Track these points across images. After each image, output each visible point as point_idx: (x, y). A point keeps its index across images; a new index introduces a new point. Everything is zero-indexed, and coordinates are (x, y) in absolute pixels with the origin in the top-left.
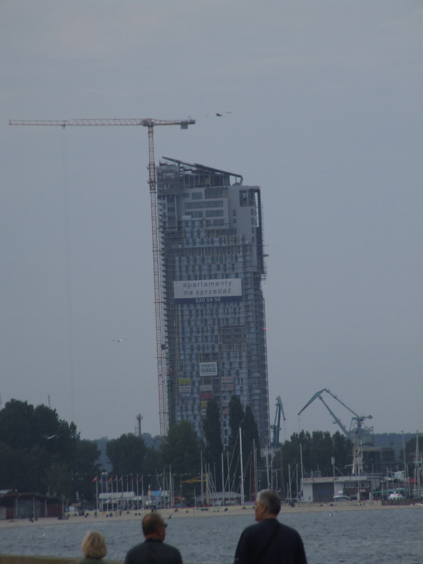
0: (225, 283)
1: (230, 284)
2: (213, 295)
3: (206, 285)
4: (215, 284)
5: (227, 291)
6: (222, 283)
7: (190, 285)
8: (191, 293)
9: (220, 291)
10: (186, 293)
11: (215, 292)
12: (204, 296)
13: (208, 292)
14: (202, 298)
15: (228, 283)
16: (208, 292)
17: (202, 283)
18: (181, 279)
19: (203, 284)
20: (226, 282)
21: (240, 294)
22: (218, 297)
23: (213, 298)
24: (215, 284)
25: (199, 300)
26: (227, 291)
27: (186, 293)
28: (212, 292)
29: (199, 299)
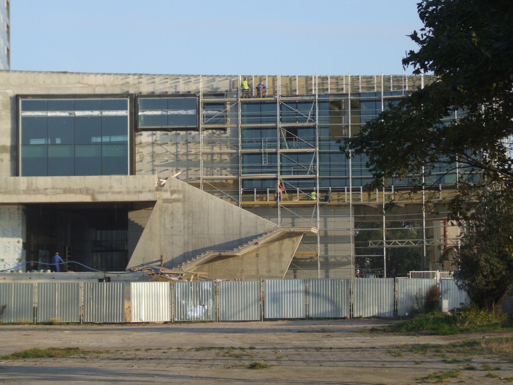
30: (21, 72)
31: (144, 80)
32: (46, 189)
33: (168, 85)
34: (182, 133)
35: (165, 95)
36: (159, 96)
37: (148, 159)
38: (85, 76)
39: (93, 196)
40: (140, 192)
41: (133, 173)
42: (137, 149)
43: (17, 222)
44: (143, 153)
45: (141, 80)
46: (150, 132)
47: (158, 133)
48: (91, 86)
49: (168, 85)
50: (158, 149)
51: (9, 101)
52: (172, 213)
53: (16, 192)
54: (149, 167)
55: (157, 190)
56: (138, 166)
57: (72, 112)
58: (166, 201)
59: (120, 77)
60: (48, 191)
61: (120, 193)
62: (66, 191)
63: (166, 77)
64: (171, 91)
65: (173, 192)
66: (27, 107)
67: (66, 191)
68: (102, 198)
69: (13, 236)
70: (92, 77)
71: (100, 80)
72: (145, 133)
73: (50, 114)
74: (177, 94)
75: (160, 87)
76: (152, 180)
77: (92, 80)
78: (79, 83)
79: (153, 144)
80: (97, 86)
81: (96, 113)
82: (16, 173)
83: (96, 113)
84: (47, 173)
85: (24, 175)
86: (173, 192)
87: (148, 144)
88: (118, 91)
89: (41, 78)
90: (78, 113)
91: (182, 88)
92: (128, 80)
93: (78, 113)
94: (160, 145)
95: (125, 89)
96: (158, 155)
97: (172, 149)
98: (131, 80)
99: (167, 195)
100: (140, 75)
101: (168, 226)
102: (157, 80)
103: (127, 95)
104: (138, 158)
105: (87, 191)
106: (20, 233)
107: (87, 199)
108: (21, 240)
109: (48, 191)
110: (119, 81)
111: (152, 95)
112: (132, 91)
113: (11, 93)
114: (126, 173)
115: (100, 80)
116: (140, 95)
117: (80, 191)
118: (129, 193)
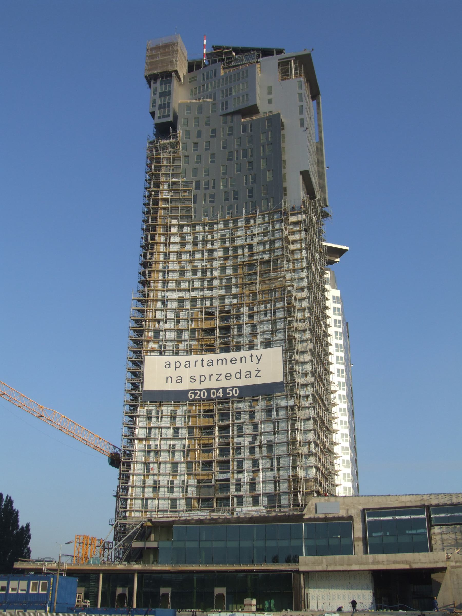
0: (248, 359)
1: (259, 361)
2: (224, 383)
3: (211, 363)
4: (229, 361)
5: (254, 374)
6: (243, 359)
7: (178, 365)
8: (180, 380)
9: (238, 376)
10: (169, 379)
11: (228, 376)
12: (206, 385)
13: (214, 378)
14: (200, 390)
15: (254, 359)
16: (214, 378)
17: (202, 360)
18: (161, 352)
19: (205, 363)
20: (251, 356)
21: (280, 379)
22: (233, 388)
23: (224, 389)
24: (229, 361)
25: (195, 394)
26: (254, 374)
27: (169, 379)
28: (223, 377)
29: (194, 392)
30: (366, 496)
31: (433, 497)
32: (383, 561)
33: (447, 499)
34: (458, 526)
35: (445, 505)
36: (442, 505)
37: (439, 542)
38: (400, 497)
39: (410, 565)
40: (437, 562)
41: (432, 551)
42: (433, 537)
43: (369, 581)
44: (436, 539)
45: (431, 497)
46: (439, 527)
47: (444, 527)
48: (403, 502)
49: (447, 499)
50: (445, 537)
51: (360, 513)
52: (457, 575)
53: (367, 563)
54: (441, 547)
55: (447, 560)
56: (434, 547)
57: (395, 517)
58: (453, 567)
59: (419, 496)
60: (385, 563)
61: (425, 563)
62: (395, 562)
63: (445, 495)
64: (448, 502)
65: (456, 562)
66: (370, 515)
67: (395, 562)
68: (415, 566)
69: (367, 589)
70: (404, 497)
71: (408, 498)
72: (435, 527)
73: (382, 518)
74: (452, 504)
75: (442, 501)
76: (443, 555)
77: (404, 498)
78: (397, 500)
79: (442, 533)
80: (407, 502)
81: (408, 517)
82: (366, 553)
83: (408, 517)
84: (383, 552)
85: (370, 554)
86: (456, 562)
87: (438, 534)
88: (418, 504)
89: (376, 499)
90: (398, 518)
91: (455, 501)
92: (423, 498)
93: (398, 518)
94: (446, 534)
95: (423, 503)
96: (445, 540)
97: (453, 536)
98: (425, 497)
99: (453, 564)
100: (430, 495)
101: (456, 583)
102: (440, 496)
103: (424, 506)
104: (433, 542)
105: (406, 562)
106: (371, 587)
107: (407, 567)
108: (372, 592)
109: (385, 563)
110: (419, 498)
111: (438, 505)
112: (426, 504)
113: (361, 508)
114: (427, 551)
115: (408, 498)
116: (431, 506)
117: (403, 562)
118: (430, 563)
